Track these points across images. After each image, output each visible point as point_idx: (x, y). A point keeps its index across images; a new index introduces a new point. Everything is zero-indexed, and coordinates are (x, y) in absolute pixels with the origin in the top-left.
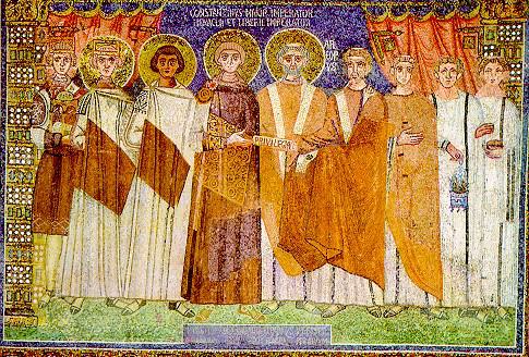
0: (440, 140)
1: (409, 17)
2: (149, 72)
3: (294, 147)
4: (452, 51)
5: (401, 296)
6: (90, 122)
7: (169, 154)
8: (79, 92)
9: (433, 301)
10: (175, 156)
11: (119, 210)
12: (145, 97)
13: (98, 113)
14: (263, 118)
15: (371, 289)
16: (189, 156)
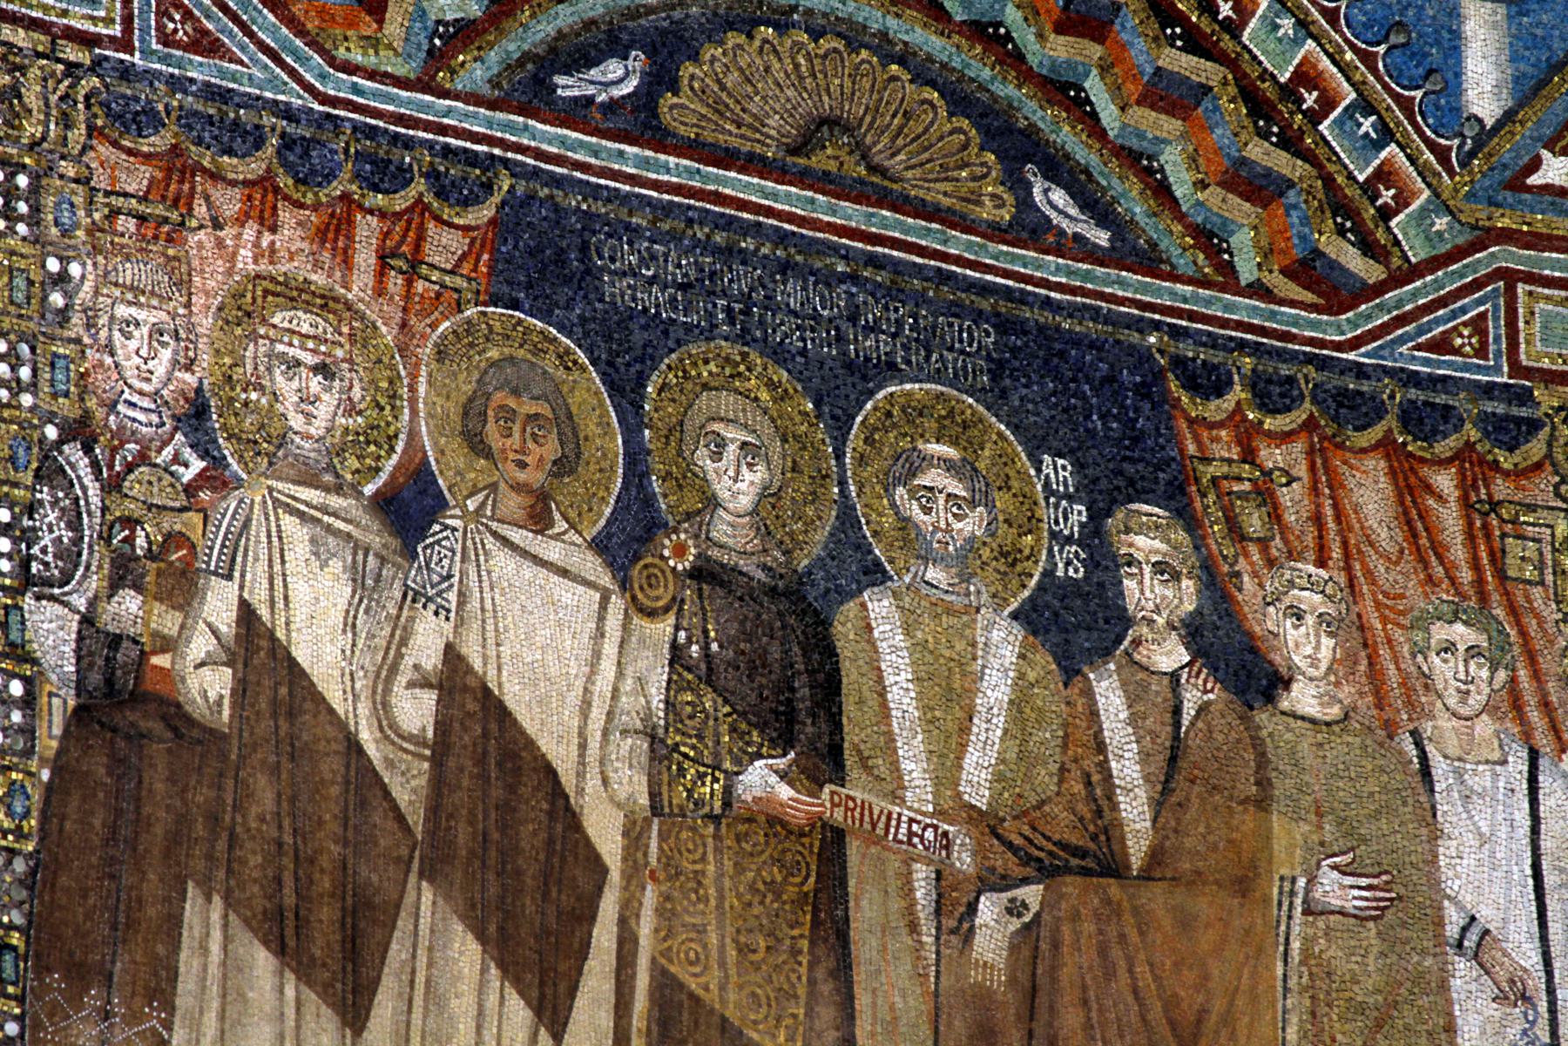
0: (1454, 921)
1: (1310, 425)
2: (458, 456)
3: (964, 860)
4: (1466, 575)
6: (246, 612)
7: (535, 806)
10: (551, 814)
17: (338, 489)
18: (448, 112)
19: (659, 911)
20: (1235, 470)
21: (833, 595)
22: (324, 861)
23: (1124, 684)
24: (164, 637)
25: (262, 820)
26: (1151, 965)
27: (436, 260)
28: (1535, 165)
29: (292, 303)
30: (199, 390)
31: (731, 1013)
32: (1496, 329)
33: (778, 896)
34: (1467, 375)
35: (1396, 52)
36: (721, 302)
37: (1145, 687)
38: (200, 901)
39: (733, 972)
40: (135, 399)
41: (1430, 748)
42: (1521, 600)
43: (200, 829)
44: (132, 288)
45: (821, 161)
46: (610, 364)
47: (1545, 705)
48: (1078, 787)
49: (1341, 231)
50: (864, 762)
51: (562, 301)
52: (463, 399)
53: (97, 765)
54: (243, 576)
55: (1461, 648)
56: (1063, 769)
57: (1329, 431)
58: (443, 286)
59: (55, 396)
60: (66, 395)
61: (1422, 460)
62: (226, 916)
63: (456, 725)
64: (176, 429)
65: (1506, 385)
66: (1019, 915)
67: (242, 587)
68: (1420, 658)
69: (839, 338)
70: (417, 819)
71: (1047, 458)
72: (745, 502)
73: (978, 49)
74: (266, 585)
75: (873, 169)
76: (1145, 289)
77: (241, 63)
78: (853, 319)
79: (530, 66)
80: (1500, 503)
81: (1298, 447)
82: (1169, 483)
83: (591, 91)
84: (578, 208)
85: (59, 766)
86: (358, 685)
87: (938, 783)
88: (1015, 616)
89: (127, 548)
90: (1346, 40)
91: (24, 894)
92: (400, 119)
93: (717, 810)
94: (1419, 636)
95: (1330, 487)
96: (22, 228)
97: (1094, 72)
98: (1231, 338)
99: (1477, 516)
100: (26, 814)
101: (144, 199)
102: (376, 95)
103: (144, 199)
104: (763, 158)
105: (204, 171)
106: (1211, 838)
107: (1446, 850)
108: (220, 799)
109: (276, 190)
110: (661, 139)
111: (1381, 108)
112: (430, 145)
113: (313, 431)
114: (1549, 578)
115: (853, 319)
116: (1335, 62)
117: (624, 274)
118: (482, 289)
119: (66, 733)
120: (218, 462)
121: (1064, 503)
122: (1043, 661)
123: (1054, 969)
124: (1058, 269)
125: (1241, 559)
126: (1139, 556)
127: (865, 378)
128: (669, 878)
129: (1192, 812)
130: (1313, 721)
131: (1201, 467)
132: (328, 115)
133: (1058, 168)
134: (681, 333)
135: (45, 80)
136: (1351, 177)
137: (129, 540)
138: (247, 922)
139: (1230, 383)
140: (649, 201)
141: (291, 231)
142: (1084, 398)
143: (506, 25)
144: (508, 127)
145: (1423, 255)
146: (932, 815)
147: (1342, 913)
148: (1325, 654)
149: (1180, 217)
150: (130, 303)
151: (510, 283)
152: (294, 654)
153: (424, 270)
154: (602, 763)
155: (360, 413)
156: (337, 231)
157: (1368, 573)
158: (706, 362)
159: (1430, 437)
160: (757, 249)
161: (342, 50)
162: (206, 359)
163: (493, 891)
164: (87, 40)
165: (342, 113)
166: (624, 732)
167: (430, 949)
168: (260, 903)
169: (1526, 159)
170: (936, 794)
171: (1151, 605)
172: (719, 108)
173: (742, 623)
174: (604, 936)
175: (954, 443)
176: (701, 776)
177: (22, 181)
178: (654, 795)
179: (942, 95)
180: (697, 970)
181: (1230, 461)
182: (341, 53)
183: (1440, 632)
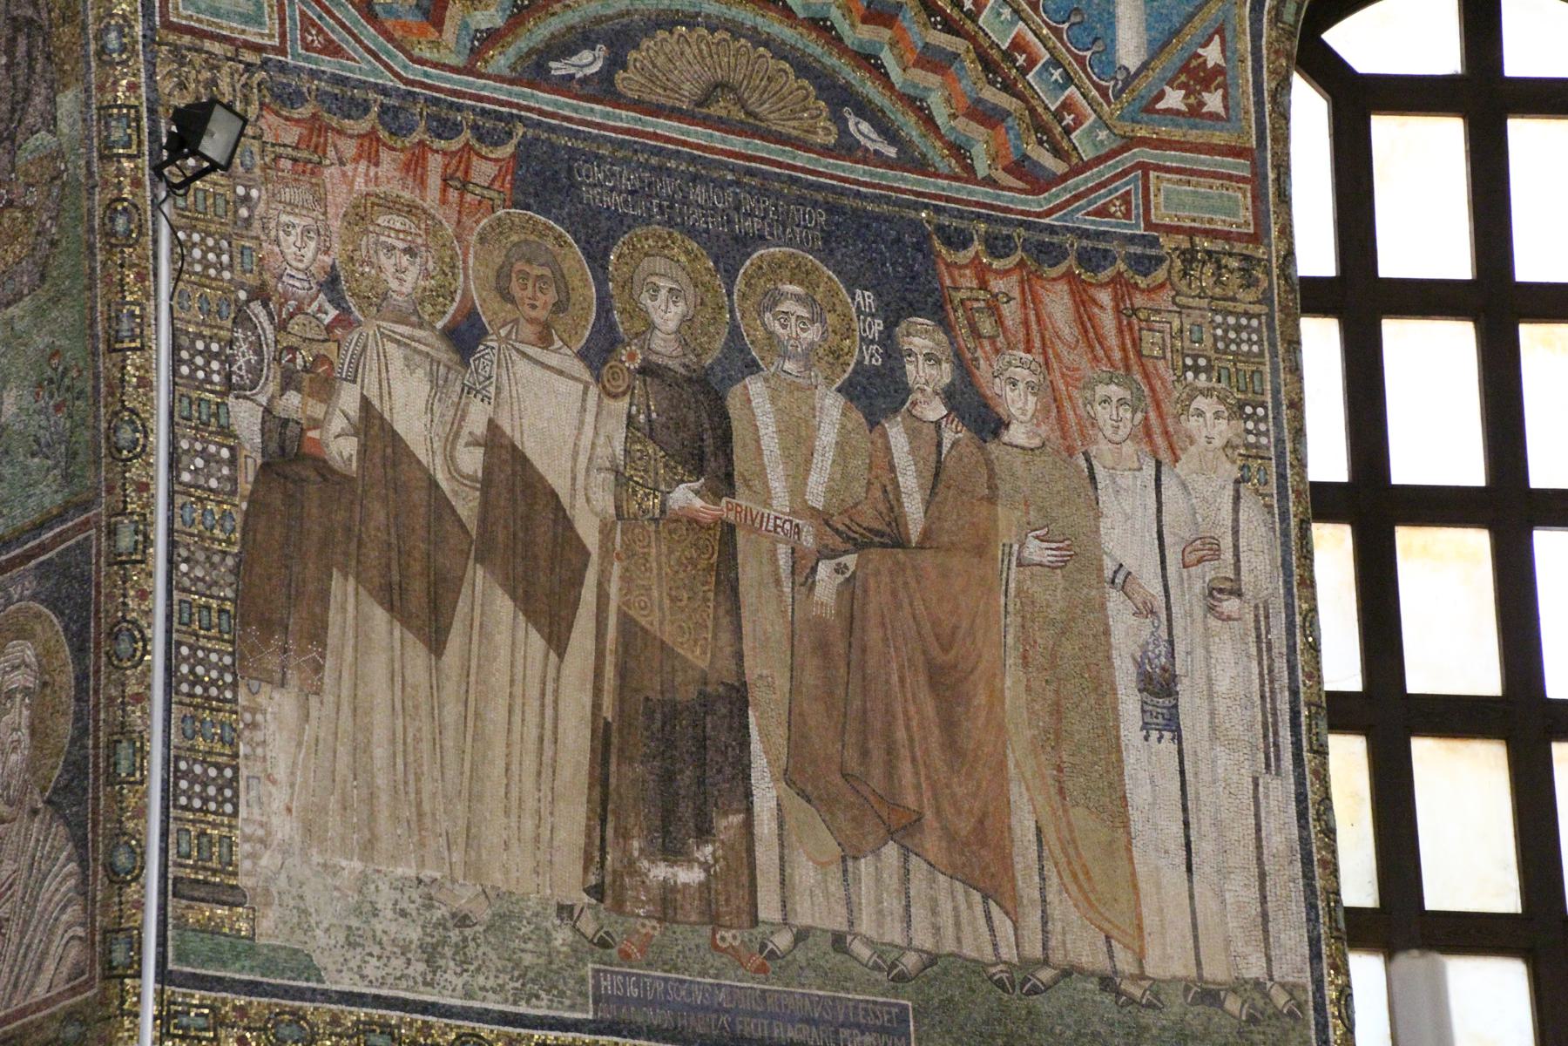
0: (1109, 567)
1: (1021, 264)
2: (495, 303)
3: (808, 540)
4: (1117, 355)
5: (1053, 943)
6: (366, 403)
9: (1125, 962)
10: (555, 521)
11: (436, 645)
13: (384, 384)
16: (588, 530)
17: (421, 326)
18: (484, 87)
19: (622, 578)
20: (975, 294)
21: (727, 381)
22: (416, 554)
23: (906, 430)
24: (315, 420)
25: (378, 529)
28: (1161, 96)
30: (333, 267)
32: (1136, 200)
34: (1118, 230)
35: (1074, 28)
36: (655, 201)
38: (341, 579)
39: (667, 613)
41: (1095, 462)
42: (1151, 369)
43: (339, 536)
44: (290, 204)
45: (717, 110)
47: (1166, 433)
48: (879, 494)
49: (1040, 142)
50: (746, 482)
51: (557, 204)
52: (496, 267)
53: (276, 499)
54: (363, 381)
55: (1114, 400)
56: (869, 483)
57: (1033, 268)
58: (483, 197)
59: (244, 272)
60: (251, 271)
61: (1091, 284)
62: (357, 589)
63: (496, 469)
64: (319, 291)
65: (1143, 236)
66: (843, 573)
67: (362, 388)
68: (1089, 407)
69: (729, 221)
70: (473, 528)
71: (858, 292)
72: (672, 325)
73: (814, 35)
74: (377, 386)
75: (748, 114)
77: (354, 60)
78: (737, 209)
79: (534, 57)
80: (1139, 309)
81: (1015, 278)
82: (935, 304)
83: (572, 70)
84: (566, 145)
86: (435, 446)
88: (839, 390)
89: (291, 365)
90: (1044, 21)
91: (232, 579)
92: (454, 93)
93: (657, 515)
94: (1088, 394)
95: (1033, 302)
97: (887, 47)
98: (972, 212)
99: (1124, 317)
100: (233, 530)
101: (296, 148)
103: (296, 148)
104: (680, 109)
105: (333, 129)
106: (960, 523)
107: (1104, 524)
109: (378, 139)
110: (617, 100)
111: (1065, 63)
112: (473, 109)
113: (404, 290)
114: (1169, 355)
115: (737, 209)
116: (1036, 35)
117: (595, 185)
118: (507, 197)
119: (256, 480)
120: (346, 311)
121: (869, 319)
122: (857, 416)
125: (979, 350)
127: (745, 246)
128: (628, 557)
130: (1023, 448)
131: (954, 294)
132: (409, 92)
133: (864, 109)
134: (631, 221)
135: (232, 74)
136: (1046, 108)
137: (293, 360)
138: (371, 594)
139: (972, 240)
140: (610, 140)
142: (881, 253)
143: (519, 31)
144: (523, 96)
145: (1091, 155)
146: (789, 514)
147: (1041, 565)
148: (1030, 407)
149: (941, 137)
150: (289, 213)
151: (524, 193)
152: (395, 427)
153: (471, 187)
154: (586, 489)
155: (433, 278)
156: (417, 164)
157: (1057, 356)
158: (647, 239)
159: (1095, 270)
160: (677, 167)
161: (417, 50)
162: (337, 246)
163: (520, 569)
164: (258, 48)
165: (418, 90)
166: (599, 470)
167: (482, 605)
168: (377, 581)
169: (1155, 93)
171: (923, 381)
172: (652, 79)
173: (671, 400)
174: (588, 594)
175: (801, 284)
176: (647, 495)
178: (618, 508)
179: (792, 66)
180: (645, 613)
181: (972, 289)
182: (416, 52)
183: (1102, 390)
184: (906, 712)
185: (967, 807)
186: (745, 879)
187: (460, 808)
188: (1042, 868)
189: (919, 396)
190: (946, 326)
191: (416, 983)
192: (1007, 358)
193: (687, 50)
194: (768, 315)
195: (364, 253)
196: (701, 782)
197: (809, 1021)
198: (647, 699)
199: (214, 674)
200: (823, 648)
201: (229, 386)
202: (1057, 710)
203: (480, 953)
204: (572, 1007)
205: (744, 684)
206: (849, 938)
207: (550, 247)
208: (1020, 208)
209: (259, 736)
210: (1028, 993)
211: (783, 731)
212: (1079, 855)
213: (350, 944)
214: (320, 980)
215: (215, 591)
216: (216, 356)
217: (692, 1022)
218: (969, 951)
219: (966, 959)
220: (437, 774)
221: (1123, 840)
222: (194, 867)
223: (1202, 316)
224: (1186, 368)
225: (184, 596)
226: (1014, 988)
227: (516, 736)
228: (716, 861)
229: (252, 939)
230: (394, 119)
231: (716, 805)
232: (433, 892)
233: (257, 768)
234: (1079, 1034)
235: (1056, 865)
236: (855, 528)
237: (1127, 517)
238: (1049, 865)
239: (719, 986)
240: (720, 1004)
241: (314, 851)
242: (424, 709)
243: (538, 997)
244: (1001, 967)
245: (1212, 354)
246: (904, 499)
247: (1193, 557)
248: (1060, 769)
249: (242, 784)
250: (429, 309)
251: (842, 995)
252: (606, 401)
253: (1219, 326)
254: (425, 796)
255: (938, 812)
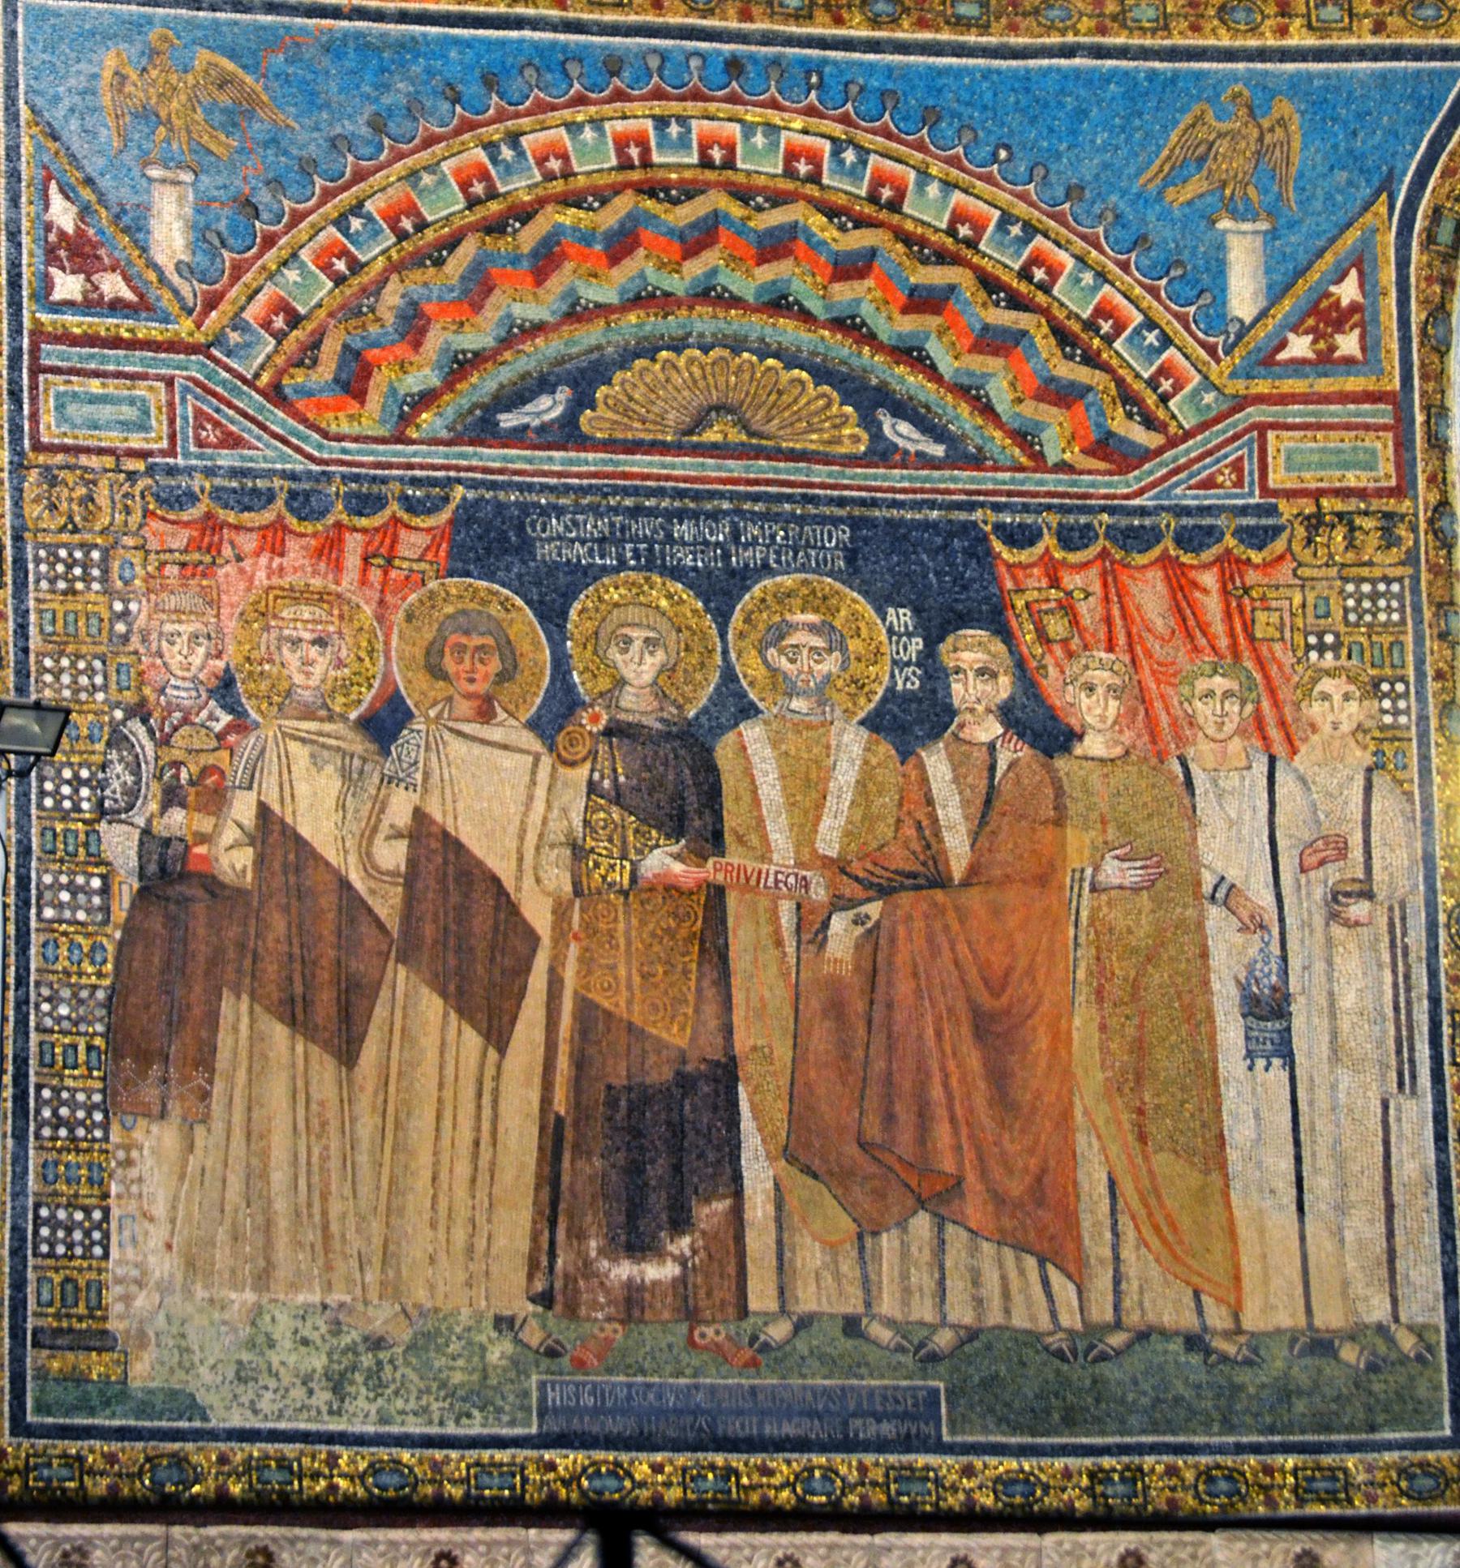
0: (1208, 880)
2: (422, 681)
3: (819, 893)
4: (1223, 643)
5: (1127, 1303)
6: (263, 810)
8: (229, 729)
9: (1217, 1317)
10: (497, 908)
11: (347, 1054)
12: (410, 742)
14: (734, 817)
15: (1046, 1283)
16: (538, 914)
17: (330, 719)
18: (415, 454)
19: (580, 960)
20: (1044, 595)
22: (324, 962)
23: (950, 756)
25: (278, 941)
26: (969, 943)
27: (407, 554)
29: (296, 600)
30: (227, 670)
31: (637, 1019)
33: (673, 938)
37: (968, 756)
38: (232, 999)
39: (637, 992)
40: (179, 683)
41: (1193, 767)
43: (231, 954)
44: (176, 611)
45: (712, 436)
46: (541, 602)
47: (1282, 724)
48: (910, 831)
50: (740, 840)
53: (156, 924)
56: (899, 821)
59: (120, 690)
61: (1192, 567)
71: (891, 610)
72: (647, 678)
73: (839, 336)
76: (973, 480)
81: (1094, 572)
85: (128, 928)
87: (798, 846)
88: (862, 723)
96: (96, 586)
100: (105, 961)
101: (186, 551)
102: (359, 452)
103: (186, 551)
104: (664, 443)
105: (230, 525)
108: (246, 933)
110: (584, 443)
112: (401, 479)
114: (1288, 635)
119: (133, 905)
122: (885, 749)
123: (891, 955)
124: (903, 478)
126: (964, 666)
127: (744, 579)
129: (1002, 836)
130: (1102, 760)
132: (324, 473)
133: (902, 409)
137: (177, 777)
138: (267, 1009)
139: (1040, 535)
141: (296, 552)
142: (922, 563)
147: (1121, 887)
157: (1149, 654)
159: (1196, 550)
162: (231, 648)
164: (143, 454)
166: (552, 846)
168: (275, 996)
170: (797, 852)
175: (816, 610)
177: (96, 555)
181: (1039, 589)
182: (333, 428)
183: (1202, 685)
184: (943, 1069)
185: (1020, 1164)
186: (731, 1269)
187: (376, 1227)
188: (1115, 1224)
189: (968, 717)
190: (1005, 634)
191: (319, 1412)
192: (1083, 661)
193: (674, 376)
194: (772, 652)
195: (263, 648)
196: (677, 1168)
197: (812, 1414)
198: (609, 1087)
199: (81, 1114)
200: (836, 1008)
201: (101, 811)
202: (1139, 1047)
203: (398, 1375)
204: (512, 1423)
205: (733, 1059)
206: (865, 1321)
207: (494, 613)
208: (1103, 491)
209: (133, 1173)
210: (1095, 1361)
211: (782, 1105)
212: (1162, 1205)
213: (239, 1379)
214: (205, 1419)
215: (83, 1028)
216: (86, 783)
217: (662, 1426)
218: (1019, 1321)
219: (1016, 1331)
220: (347, 1192)
221: (1219, 1183)
222: (57, 1316)
223: (1331, 588)
224: (1308, 648)
225: (47, 1037)
226: (1076, 1357)
227: (446, 1142)
228: (694, 1252)
229: (124, 1382)
230: (304, 503)
231: (696, 1192)
232: (341, 1317)
233: (132, 1206)
234: (1157, 1400)
235: (1133, 1218)
236: (878, 871)
237: (1231, 823)
238: (1124, 1220)
239: (697, 1387)
240: (698, 1406)
241: (199, 1286)
242: (334, 1125)
243: (469, 1416)
244: (1060, 1335)
245: (1342, 629)
246: (946, 835)
247: (1314, 859)
248: (1140, 1112)
249: (114, 1225)
250: (341, 700)
251: (855, 1382)
252: (561, 770)
253: (1350, 596)
254: (333, 1214)
255: (983, 1173)
